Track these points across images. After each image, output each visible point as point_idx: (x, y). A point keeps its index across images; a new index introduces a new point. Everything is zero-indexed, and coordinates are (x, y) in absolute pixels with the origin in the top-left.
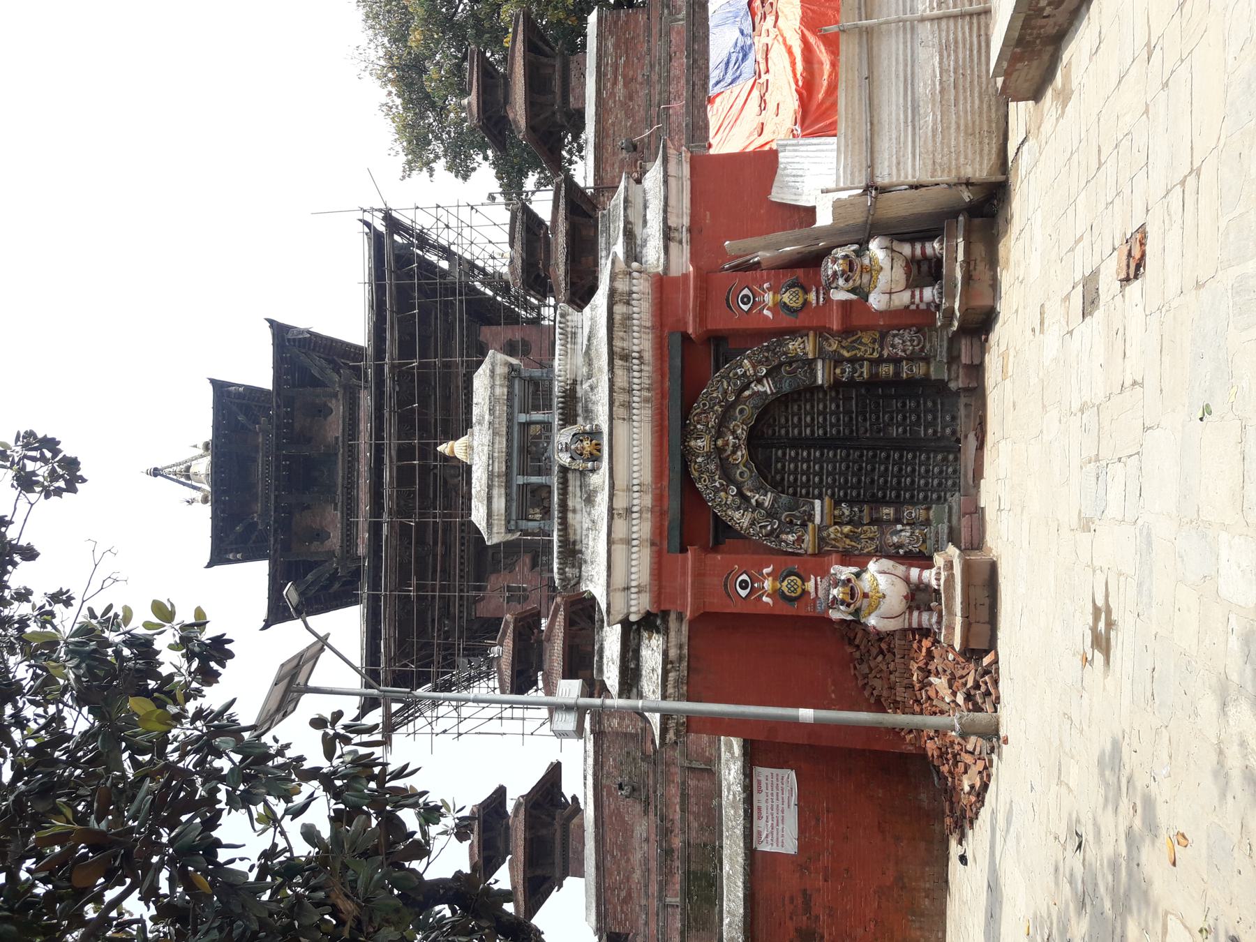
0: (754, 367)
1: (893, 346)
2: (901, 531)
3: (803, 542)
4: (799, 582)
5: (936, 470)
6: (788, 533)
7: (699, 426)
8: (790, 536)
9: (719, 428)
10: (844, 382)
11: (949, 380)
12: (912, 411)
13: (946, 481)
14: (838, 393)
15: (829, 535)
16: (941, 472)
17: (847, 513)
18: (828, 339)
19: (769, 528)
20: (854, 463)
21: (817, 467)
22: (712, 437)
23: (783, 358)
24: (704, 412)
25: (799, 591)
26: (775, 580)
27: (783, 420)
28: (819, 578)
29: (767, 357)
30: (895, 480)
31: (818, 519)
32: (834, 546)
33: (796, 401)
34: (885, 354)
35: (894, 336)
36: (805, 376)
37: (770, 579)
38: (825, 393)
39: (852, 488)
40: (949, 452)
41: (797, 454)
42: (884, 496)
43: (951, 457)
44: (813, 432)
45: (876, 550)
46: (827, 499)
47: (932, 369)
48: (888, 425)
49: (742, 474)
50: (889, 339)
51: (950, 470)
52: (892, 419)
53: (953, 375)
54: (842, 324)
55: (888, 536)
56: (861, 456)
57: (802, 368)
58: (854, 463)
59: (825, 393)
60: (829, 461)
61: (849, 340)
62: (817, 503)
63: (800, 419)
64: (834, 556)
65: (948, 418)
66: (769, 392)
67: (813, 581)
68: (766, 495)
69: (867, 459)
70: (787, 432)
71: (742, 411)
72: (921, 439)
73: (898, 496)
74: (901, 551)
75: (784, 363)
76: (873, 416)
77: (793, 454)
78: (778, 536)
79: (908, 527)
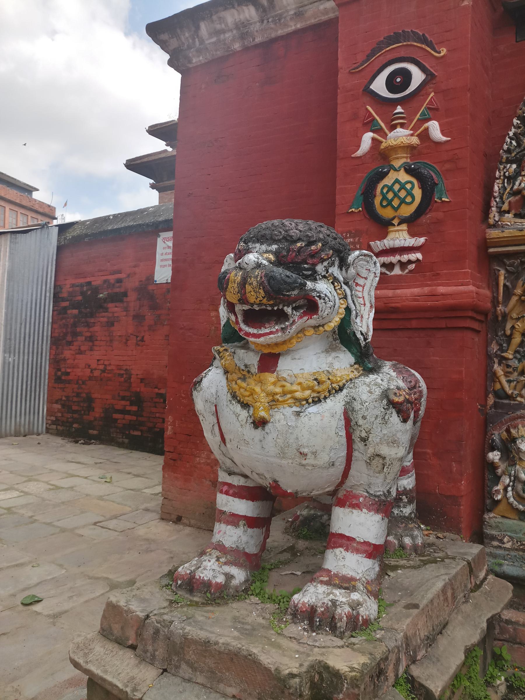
4: (407, 211)
25: (387, 213)
26: (410, 148)
28: (419, 256)
32: (508, 293)
37: (415, 140)
45: (501, 395)
64: (486, 292)
67: (410, 242)
74: (494, 456)
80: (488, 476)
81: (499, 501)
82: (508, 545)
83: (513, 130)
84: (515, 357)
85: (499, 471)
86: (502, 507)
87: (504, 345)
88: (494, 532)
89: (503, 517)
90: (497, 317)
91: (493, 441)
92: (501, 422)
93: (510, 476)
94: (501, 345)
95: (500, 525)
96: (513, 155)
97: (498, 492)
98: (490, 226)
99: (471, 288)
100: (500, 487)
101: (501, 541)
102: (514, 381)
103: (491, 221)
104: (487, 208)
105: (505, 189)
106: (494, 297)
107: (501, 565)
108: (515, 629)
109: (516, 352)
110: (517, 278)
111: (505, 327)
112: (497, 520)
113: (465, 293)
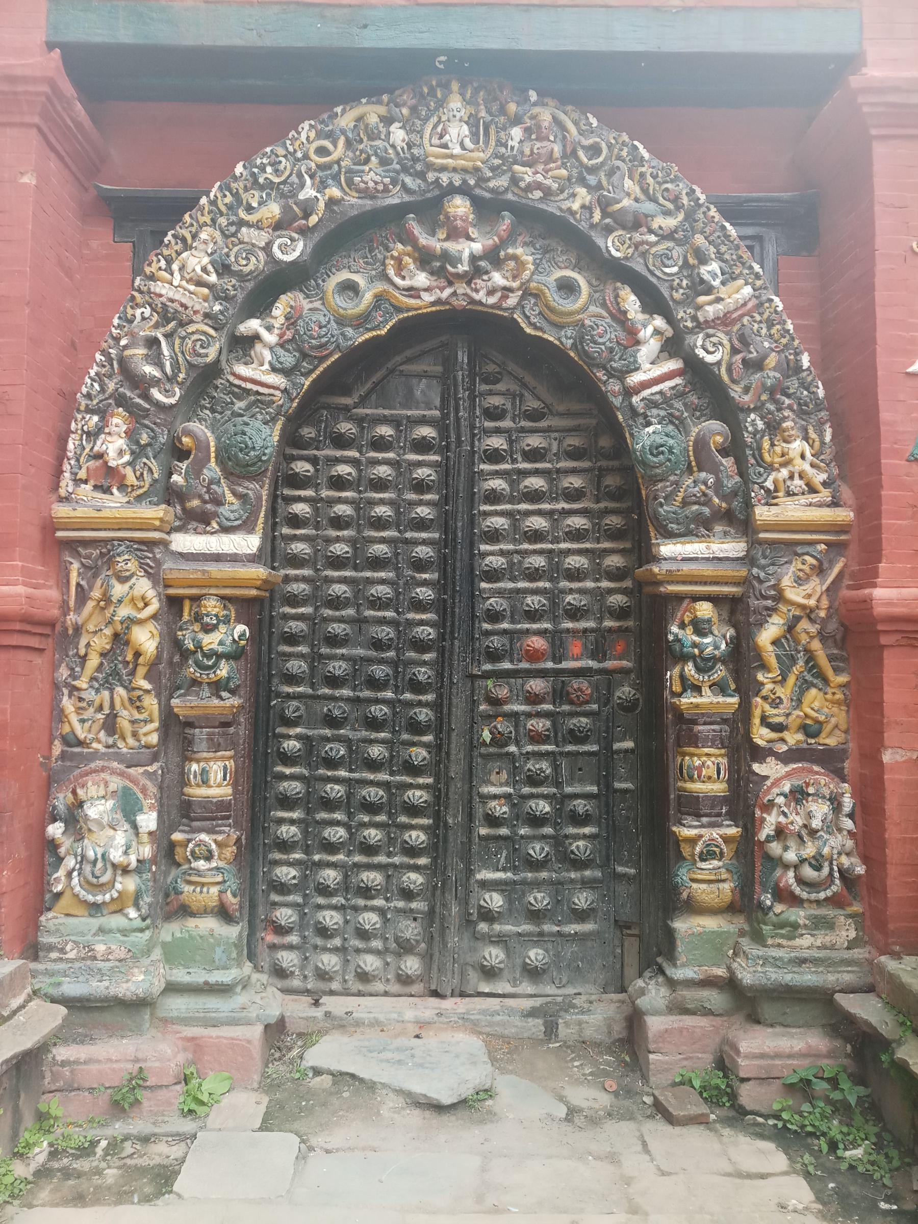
0: (725, 321)
1: (798, 795)
2: (135, 827)
3: (107, 490)
5: (370, 919)
6: (131, 435)
7: (517, 133)
8: (120, 443)
9: (511, 207)
10: (666, 632)
11: (672, 984)
12: (558, 842)
13: (336, 950)
14: (621, 613)
15: (123, 580)
16: (363, 934)
17: (211, 641)
18: (820, 570)
19: (149, 370)
20: (394, 664)
21: (380, 549)
22: (482, 180)
23: (755, 422)
24: (570, 154)
27: (535, 441)
29: (757, 365)
30: (336, 791)
31: (184, 542)
32: (82, 596)
33: (596, 476)
34: (769, 769)
35: (835, 802)
36: (685, 503)
38: (617, 575)
39: (315, 659)
40: (427, 958)
41: (420, 487)
42: (287, 759)
43: (412, 965)
44: (494, 536)
45: (71, 741)
46: (260, 572)
47: (710, 923)
48: (514, 771)
49: (350, 288)
50: (823, 781)
51: (370, 963)
52: (533, 780)
53: (690, 996)
54: (893, 619)
55: (116, 783)
56: (417, 687)
57: (718, 485)
58: (394, 664)
59: (617, 575)
60: (401, 586)
61: (816, 645)
62: (250, 543)
63: (534, 496)
64: (53, 594)
65: (535, 955)
66: (635, 378)
68: (274, 369)
69: (410, 704)
70: (494, 456)
71: (567, 288)
72: (470, 873)
73: (286, 802)
74: (55, 830)
75: (736, 429)
76: (541, 725)
77: (422, 473)
78: (121, 401)
79: (147, 851)
80: (49, 859)
81: (59, 895)
82: (72, 955)
83: (96, 368)
84: (91, 687)
85: (62, 851)
86: (64, 902)
87: (78, 669)
88: (52, 940)
89: (67, 915)
90: (67, 629)
91: (54, 807)
92: (69, 779)
93: (76, 856)
94: (72, 669)
95: (61, 928)
96: (95, 402)
97: (57, 880)
98: (61, 500)
99: (20, 589)
100: (61, 873)
101: (62, 951)
102: (88, 720)
103: (62, 492)
104: (59, 472)
105: (84, 448)
106: (64, 601)
107: (59, 984)
108: (72, 1072)
109: (93, 679)
110: (95, 576)
111: (78, 643)
112: (56, 921)
113: (11, 596)
